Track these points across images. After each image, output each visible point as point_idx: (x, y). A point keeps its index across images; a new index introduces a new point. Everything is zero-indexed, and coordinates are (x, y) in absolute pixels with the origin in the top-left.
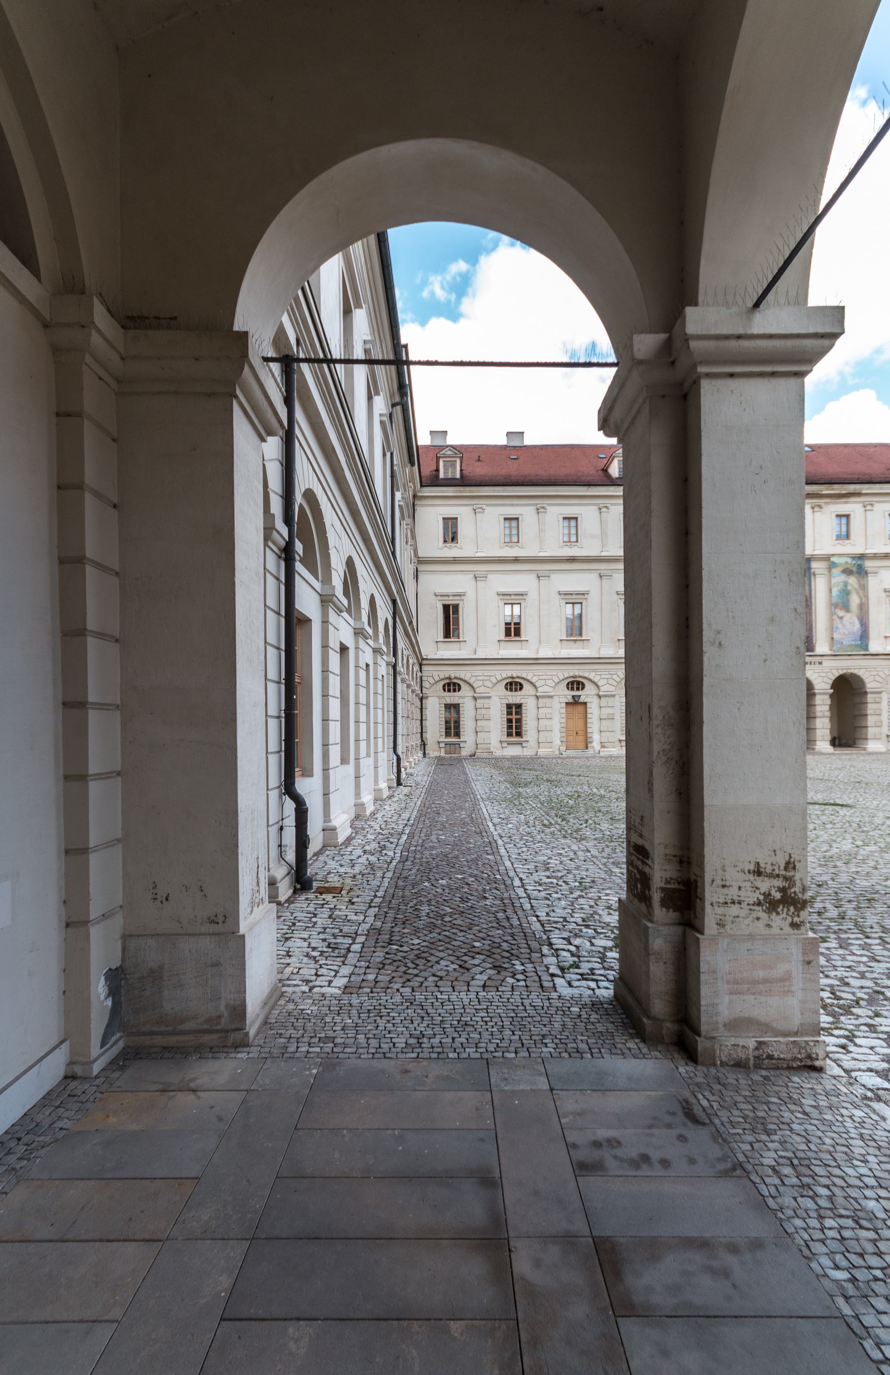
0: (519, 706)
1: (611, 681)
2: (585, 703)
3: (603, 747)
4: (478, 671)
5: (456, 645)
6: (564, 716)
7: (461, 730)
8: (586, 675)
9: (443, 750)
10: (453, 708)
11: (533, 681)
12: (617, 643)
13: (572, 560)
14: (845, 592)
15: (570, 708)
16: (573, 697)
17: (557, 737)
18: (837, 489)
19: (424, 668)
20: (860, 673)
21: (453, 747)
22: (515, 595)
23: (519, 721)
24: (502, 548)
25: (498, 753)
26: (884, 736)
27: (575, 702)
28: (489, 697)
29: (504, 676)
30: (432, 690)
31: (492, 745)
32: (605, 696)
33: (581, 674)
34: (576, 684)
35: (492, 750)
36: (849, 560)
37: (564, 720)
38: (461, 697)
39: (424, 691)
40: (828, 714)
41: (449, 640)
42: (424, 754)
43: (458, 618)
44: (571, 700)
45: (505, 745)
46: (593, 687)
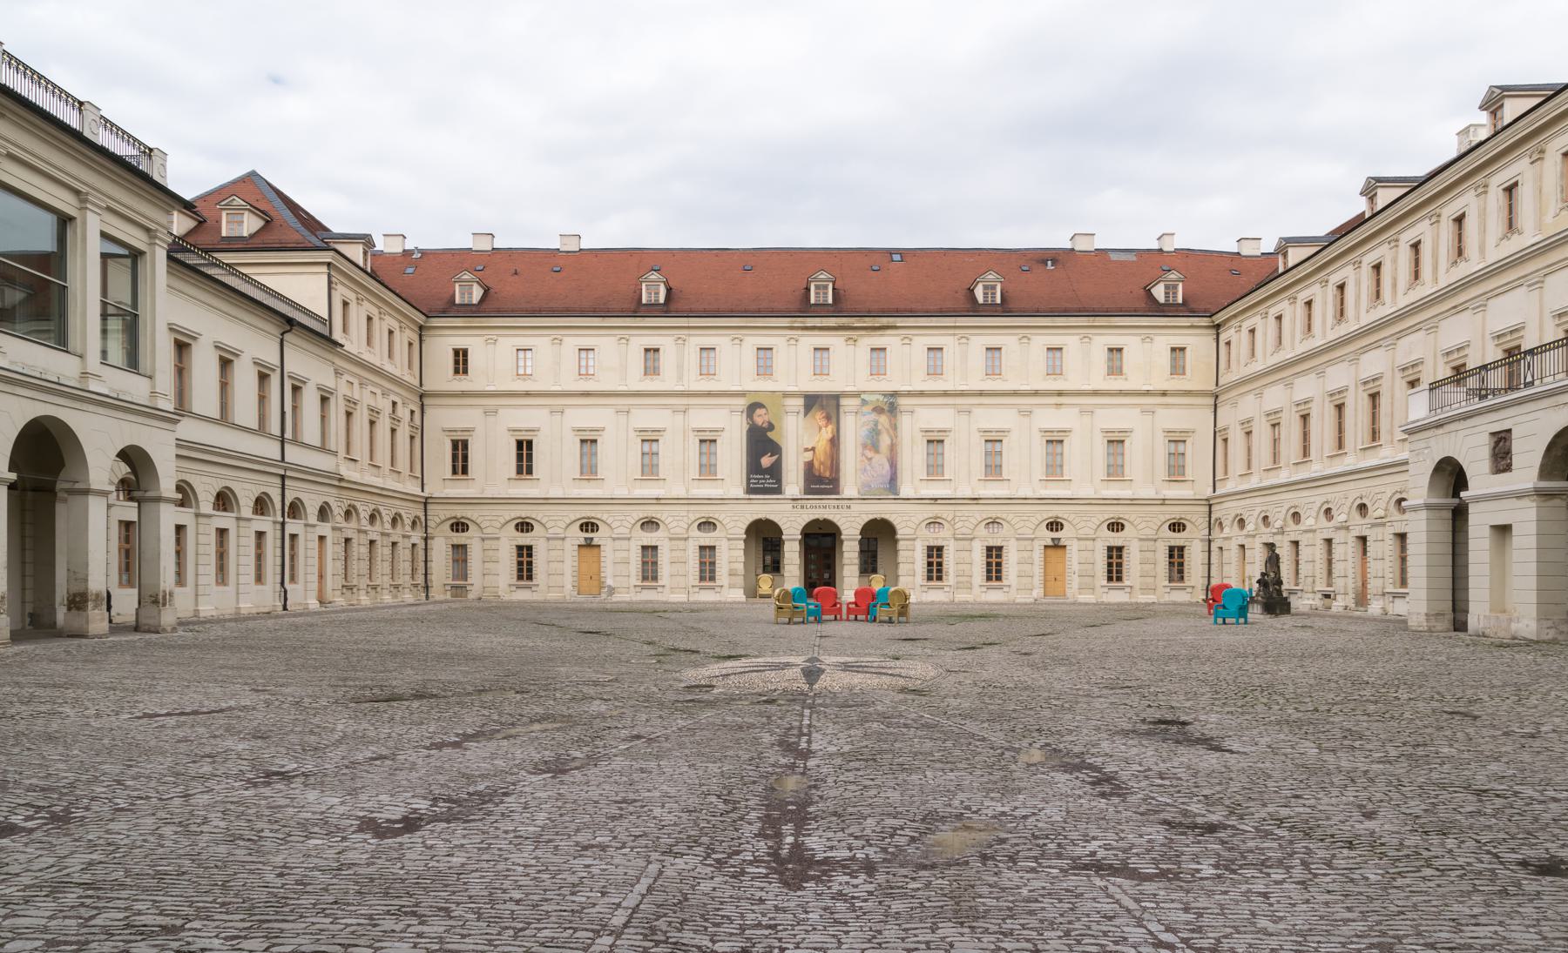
0: (530, 548)
1: (625, 523)
8: (599, 516)
9: (449, 593)
10: (460, 551)
14: (875, 432)
15: (585, 551)
16: (586, 539)
17: (568, 582)
18: (869, 322)
19: (429, 507)
21: (459, 591)
23: (530, 563)
24: (513, 380)
25: (507, 597)
26: (918, 587)
27: (589, 545)
28: (498, 539)
29: (513, 516)
32: (618, 539)
33: (593, 515)
34: (589, 526)
35: (500, 593)
36: (881, 398)
37: (576, 564)
39: (429, 530)
40: (857, 561)
42: (427, 597)
43: (531, 454)
44: (583, 543)
45: (514, 588)
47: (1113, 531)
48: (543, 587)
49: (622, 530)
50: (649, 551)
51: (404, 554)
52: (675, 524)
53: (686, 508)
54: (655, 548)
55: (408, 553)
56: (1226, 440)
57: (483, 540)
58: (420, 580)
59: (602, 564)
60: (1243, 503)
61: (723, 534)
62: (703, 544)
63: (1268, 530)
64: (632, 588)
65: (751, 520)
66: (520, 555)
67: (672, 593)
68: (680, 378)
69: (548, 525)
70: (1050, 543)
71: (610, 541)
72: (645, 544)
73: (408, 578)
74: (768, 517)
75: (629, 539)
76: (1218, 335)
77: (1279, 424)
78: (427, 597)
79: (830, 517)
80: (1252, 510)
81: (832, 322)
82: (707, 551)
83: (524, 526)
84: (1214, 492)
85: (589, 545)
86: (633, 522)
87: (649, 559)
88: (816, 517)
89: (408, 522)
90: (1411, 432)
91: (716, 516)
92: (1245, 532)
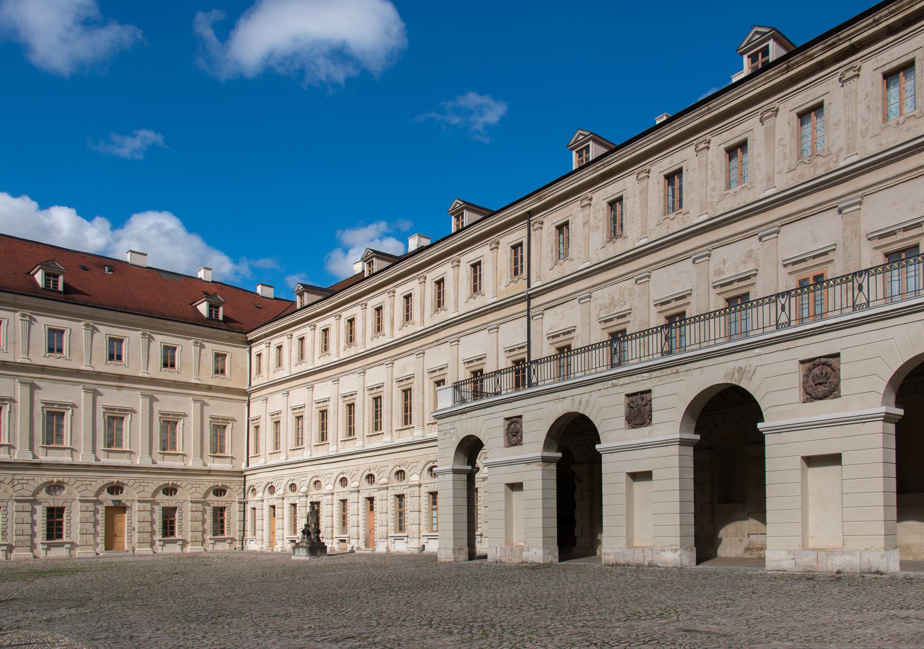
47: (167, 495)
56: (257, 427)
60: (273, 474)
63: (295, 494)
70: (112, 504)
76: (251, 348)
77: (302, 416)
80: (282, 479)
84: (248, 466)
90: (438, 417)
92: (275, 495)
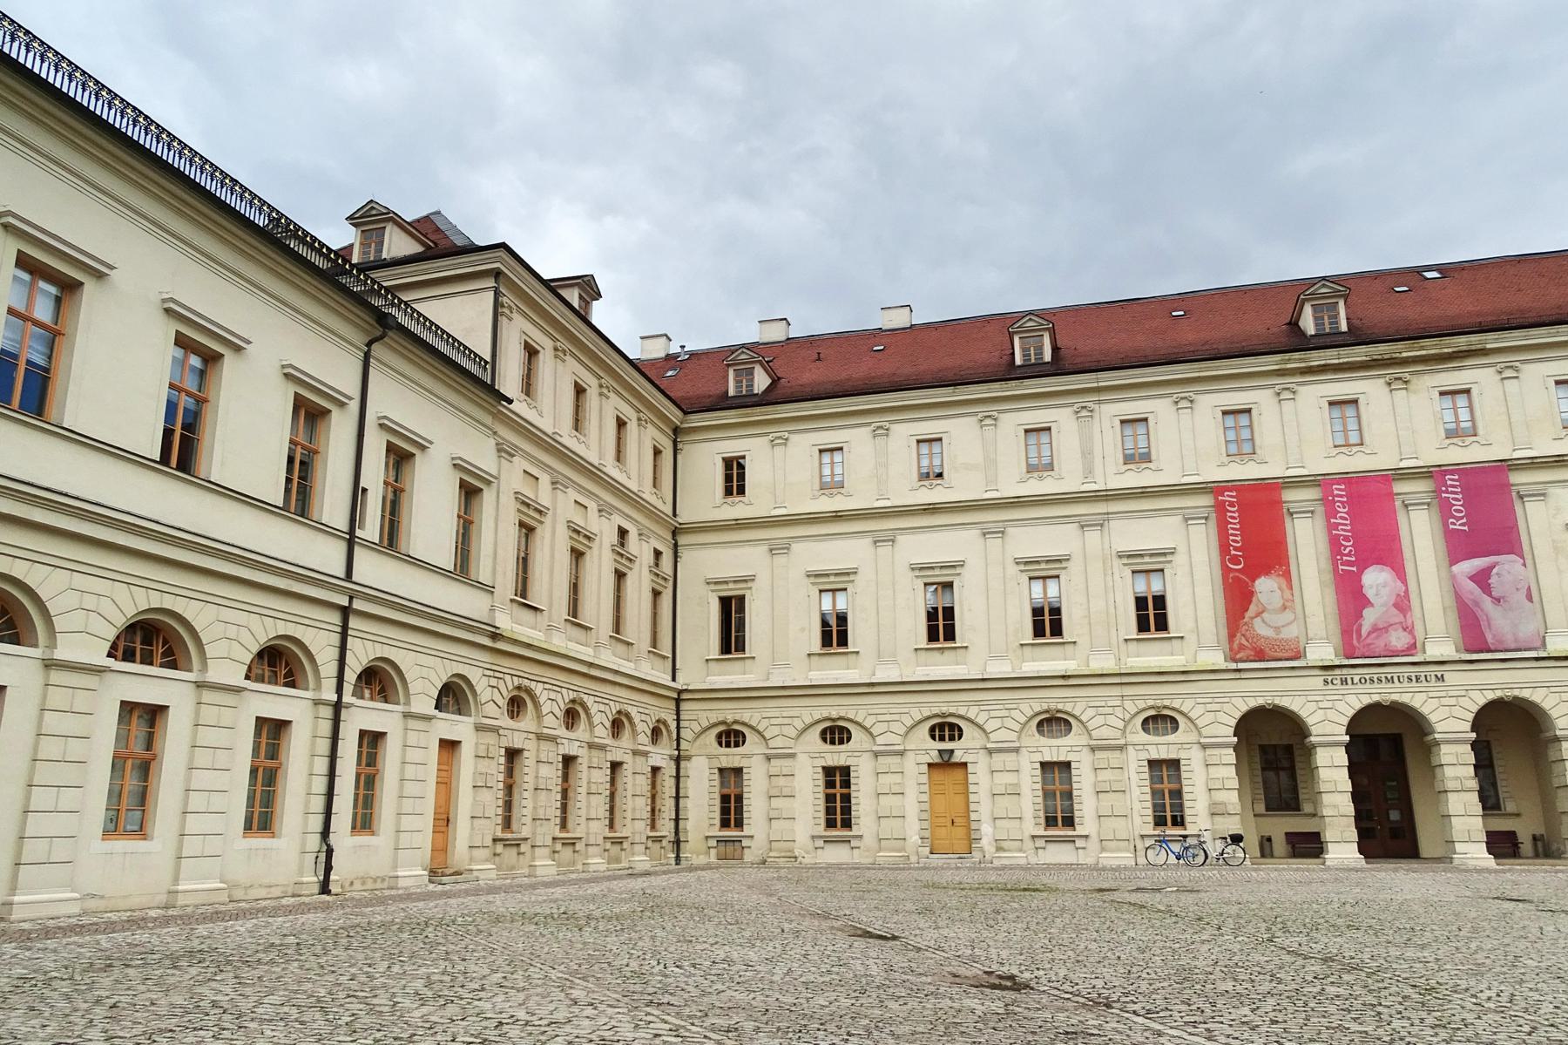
0: (846, 771)
1: (1009, 723)
2: (964, 765)
3: (999, 849)
4: (772, 709)
5: (738, 664)
6: (926, 788)
7: (745, 815)
8: (962, 711)
9: (713, 852)
10: (732, 775)
11: (867, 724)
12: (1019, 652)
13: (932, 509)
15: (939, 775)
17: (913, 831)
18: (1430, 347)
19: (683, 706)
20: (1536, 697)
21: (730, 847)
22: (836, 575)
23: (847, 798)
27: (945, 764)
28: (792, 756)
29: (817, 716)
30: (698, 742)
31: (797, 845)
32: (1000, 750)
33: (952, 710)
34: (946, 730)
37: (925, 797)
38: (744, 756)
39: (684, 745)
41: (730, 656)
42: (678, 859)
44: (937, 760)
45: (820, 843)
46: (977, 733)
48: (869, 840)
49: (1002, 735)
50: (1056, 771)
51: (634, 783)
52: (1099, 720)
53: (1117, 691)
54: (1066, 766)
55: (643, 783)
57: (768, 758)
58: (666, 828)
59: (972, 798)
61: (1193, 737)
62: (1155, 756)
64: (1029, 844)
65: (1245, 709)
66: (830, 784)
67: (1103, 850)
68: (1089, 472)
69: (875, 731)
71: (982, 755)
72: (1048, 758)
73: (642, 827)
74: (1277, 701)
75: (1017, 750)
78: (678, 859)
79: (1405, 699)
81: (1359, 353)
82: (1165, 770)
83: (836, 734)
85: (945, 764)
86: (1023, 719)
87: (1058, 786)
88: (1376, 698)
89: (644, 729)
91: (1176, 704)
